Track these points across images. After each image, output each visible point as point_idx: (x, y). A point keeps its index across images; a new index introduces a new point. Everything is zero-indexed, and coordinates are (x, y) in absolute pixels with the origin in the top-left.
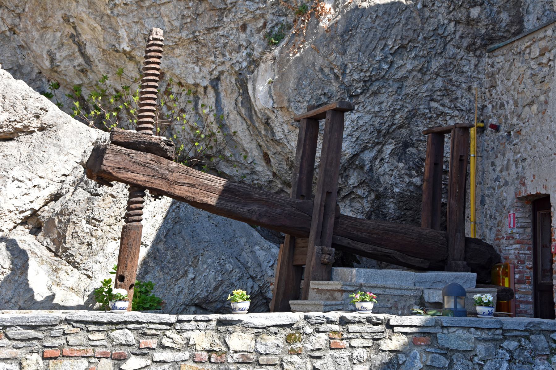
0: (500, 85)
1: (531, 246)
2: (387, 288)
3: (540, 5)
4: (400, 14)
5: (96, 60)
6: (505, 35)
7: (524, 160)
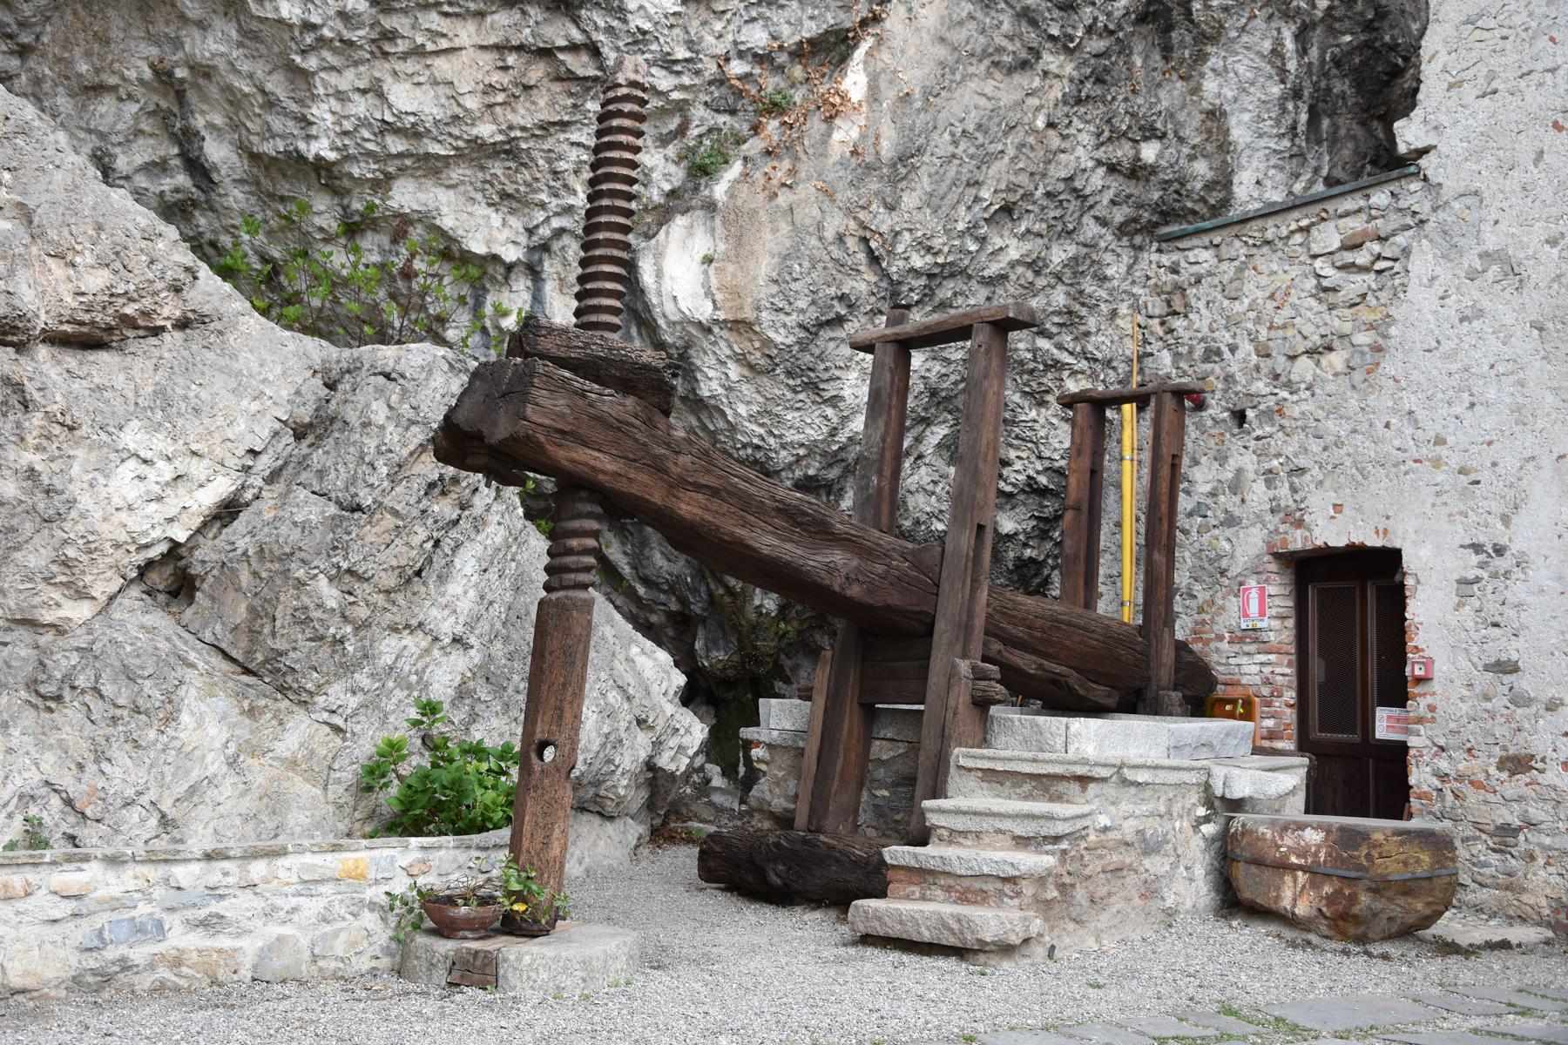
0: (1204, 311)
1: (1293, 658)
2: (1162, 768)
4: (1006, 134)
5: (227, 180)
6: (1197, 208)
7: (1301, 471)
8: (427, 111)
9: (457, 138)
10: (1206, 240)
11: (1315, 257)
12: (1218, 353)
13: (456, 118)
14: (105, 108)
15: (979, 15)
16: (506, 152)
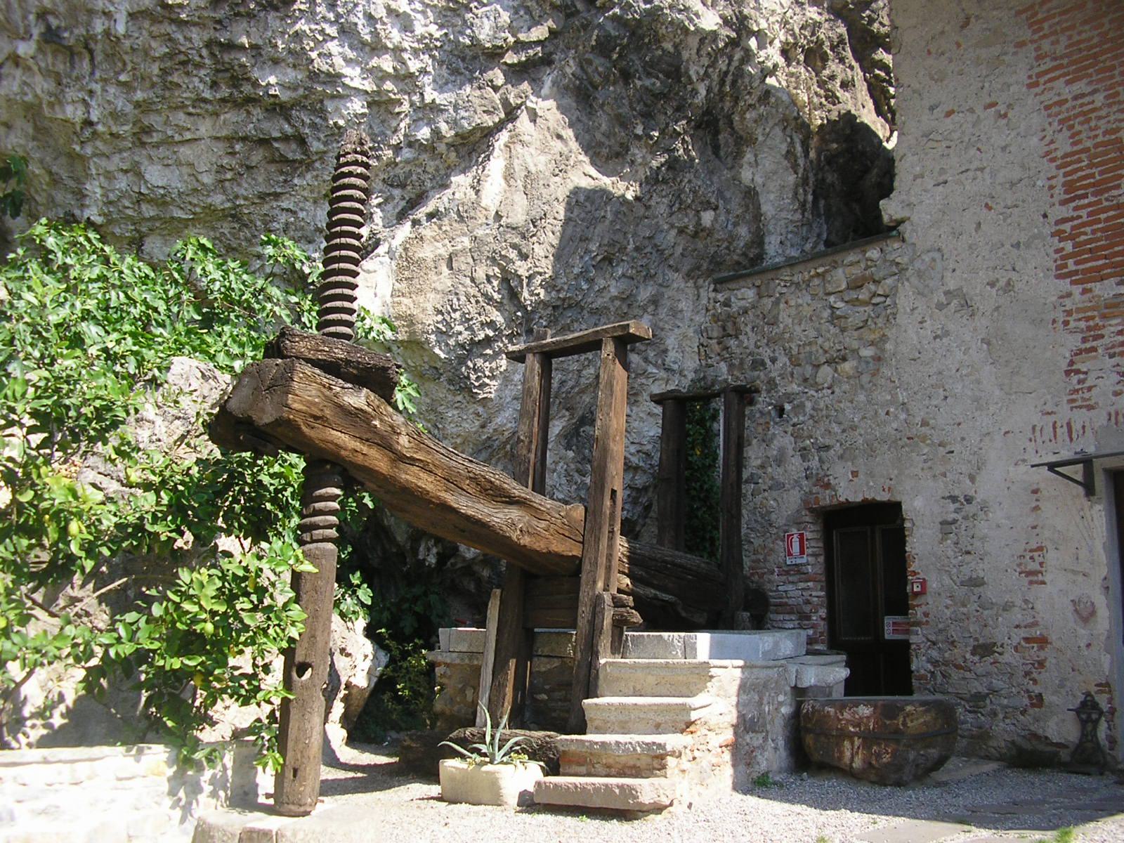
0: (750, 333)
3: (783, 222)
4: (606, 204)
8: (173, 185)
9: (195, 206)
10: (749, 281)
11: (830, 294)
12: (763, 363)
13: (195, 190)
15: (584, 119)
16: (233, 216)
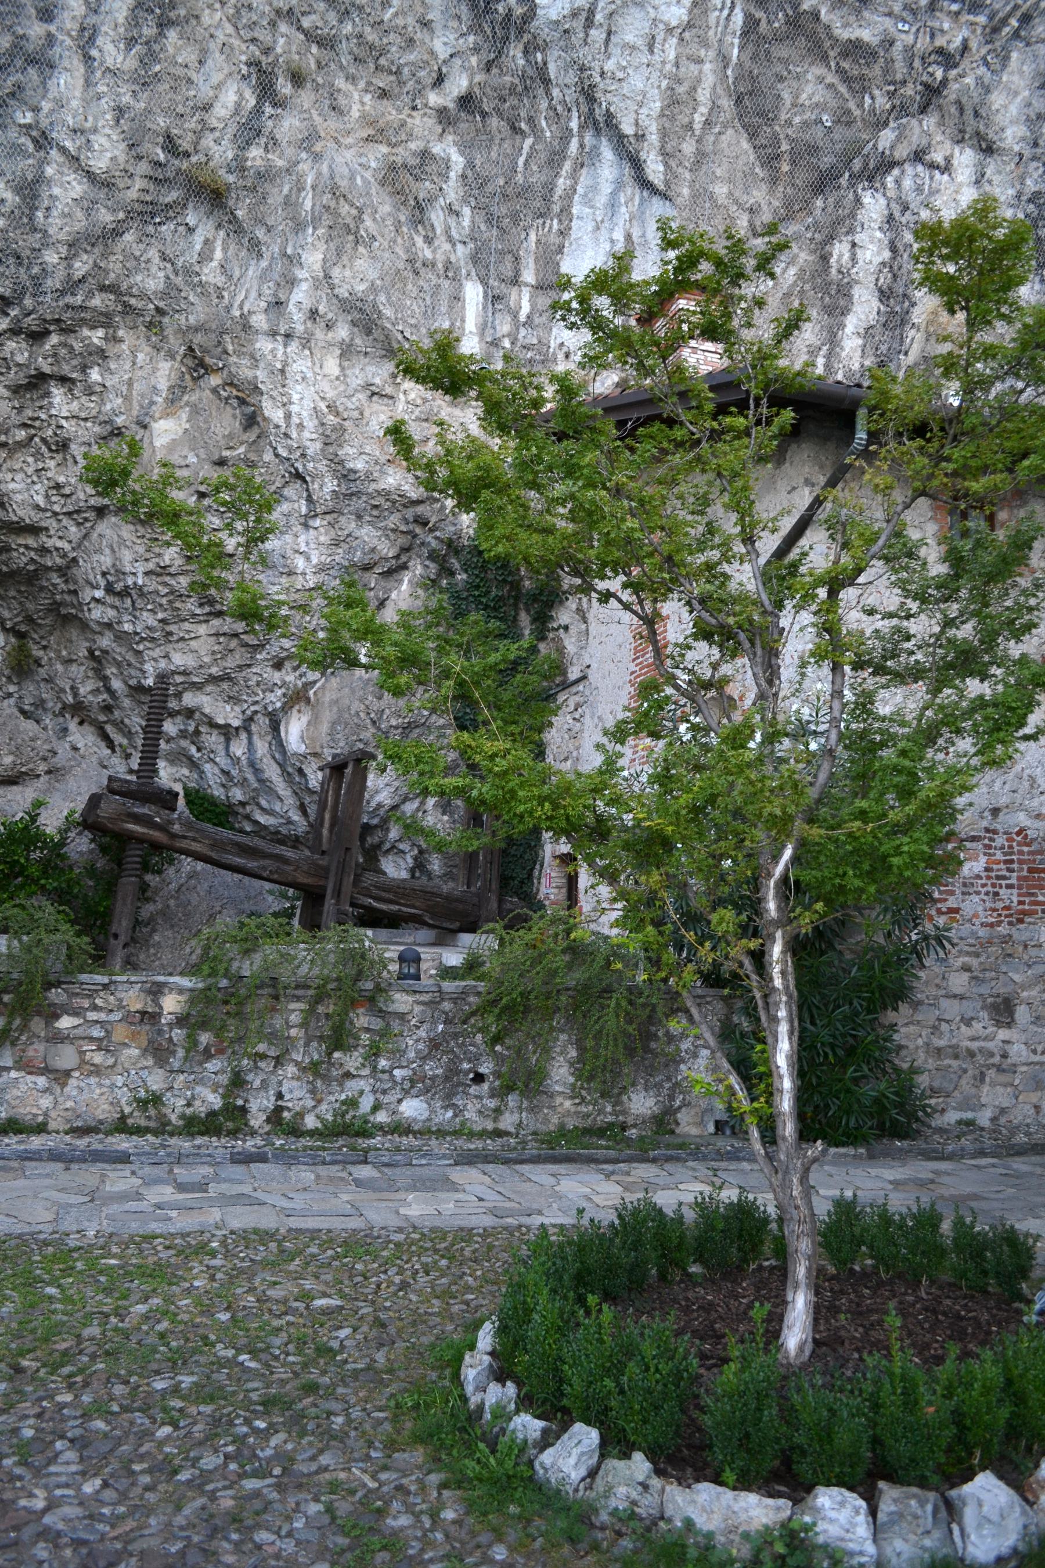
14: (74, 668)
